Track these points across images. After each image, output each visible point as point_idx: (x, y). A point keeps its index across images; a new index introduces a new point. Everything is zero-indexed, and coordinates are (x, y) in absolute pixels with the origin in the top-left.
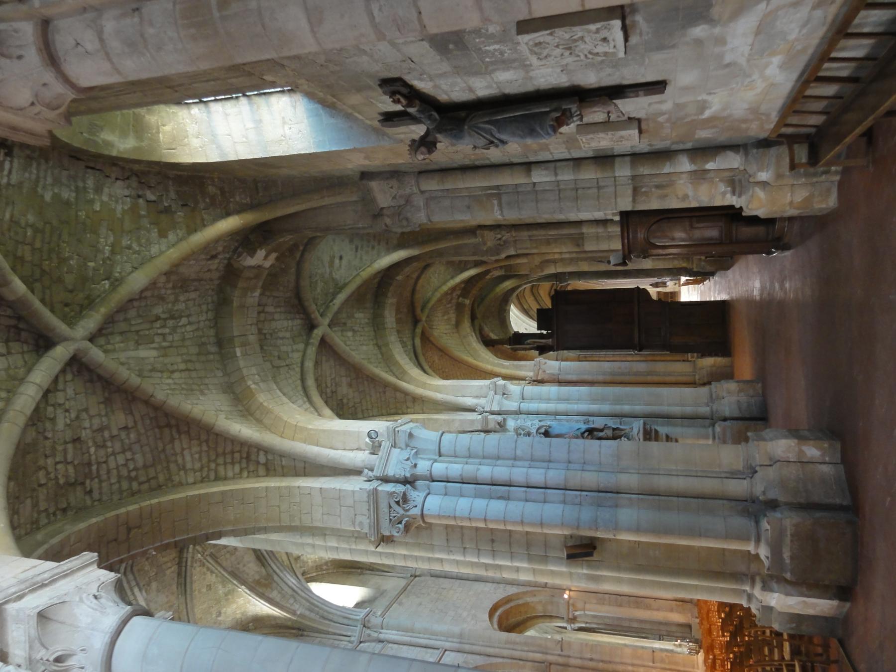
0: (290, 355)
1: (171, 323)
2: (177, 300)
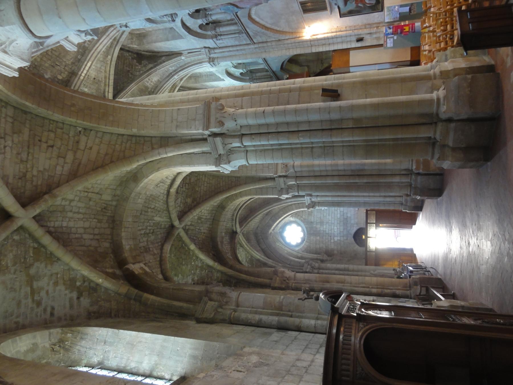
0: (77, 199)
1: (148, 232)
2: (147, 241)
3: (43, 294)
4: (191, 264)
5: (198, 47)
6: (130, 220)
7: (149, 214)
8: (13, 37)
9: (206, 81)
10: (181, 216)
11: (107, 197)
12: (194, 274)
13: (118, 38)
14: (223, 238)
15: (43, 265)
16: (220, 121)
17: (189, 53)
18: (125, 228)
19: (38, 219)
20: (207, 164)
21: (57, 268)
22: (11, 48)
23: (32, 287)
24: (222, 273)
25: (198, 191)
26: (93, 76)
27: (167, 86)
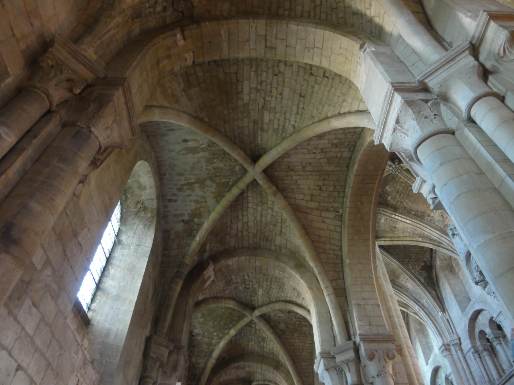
0: (275, 214)
1: (247, 282)
2: (237, 283)
3: (189, 192)
4: (215, 332)
5: (457, 331)
6: (258, 264)
7: (265, 283)
8: (409, 133)
9: (421, 342)
10: (264, 318)
11: (278, 240)
12: (204, 336)
13: (442, 246)
14: (243, 368)
15: (213, 190)
16: (374, 355)
17: (448, 320)
18: (249, 259)
19: (254, 183)
20: (322, 342)
21: (211, 201)
22: (399, 134)
23: (195, 183)
24: (204, 369)
25: (293, 336)
26: (397, 226)
27: (404, 298)
